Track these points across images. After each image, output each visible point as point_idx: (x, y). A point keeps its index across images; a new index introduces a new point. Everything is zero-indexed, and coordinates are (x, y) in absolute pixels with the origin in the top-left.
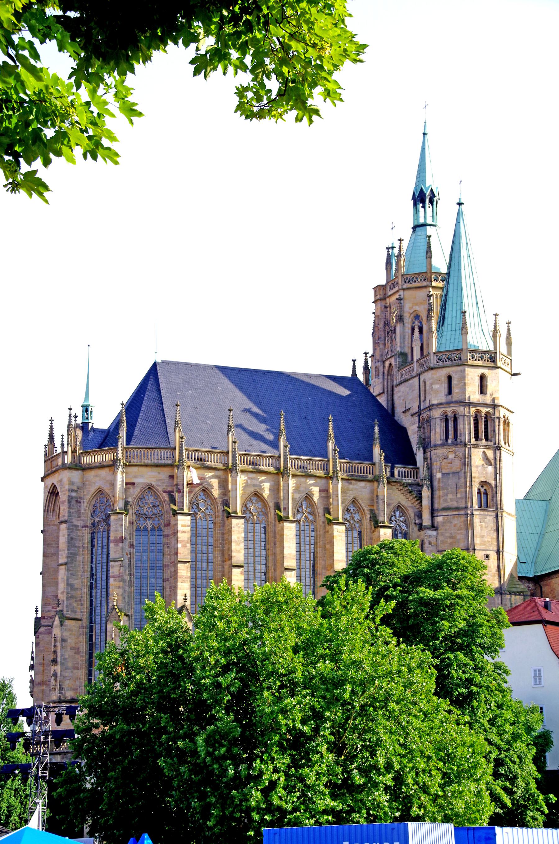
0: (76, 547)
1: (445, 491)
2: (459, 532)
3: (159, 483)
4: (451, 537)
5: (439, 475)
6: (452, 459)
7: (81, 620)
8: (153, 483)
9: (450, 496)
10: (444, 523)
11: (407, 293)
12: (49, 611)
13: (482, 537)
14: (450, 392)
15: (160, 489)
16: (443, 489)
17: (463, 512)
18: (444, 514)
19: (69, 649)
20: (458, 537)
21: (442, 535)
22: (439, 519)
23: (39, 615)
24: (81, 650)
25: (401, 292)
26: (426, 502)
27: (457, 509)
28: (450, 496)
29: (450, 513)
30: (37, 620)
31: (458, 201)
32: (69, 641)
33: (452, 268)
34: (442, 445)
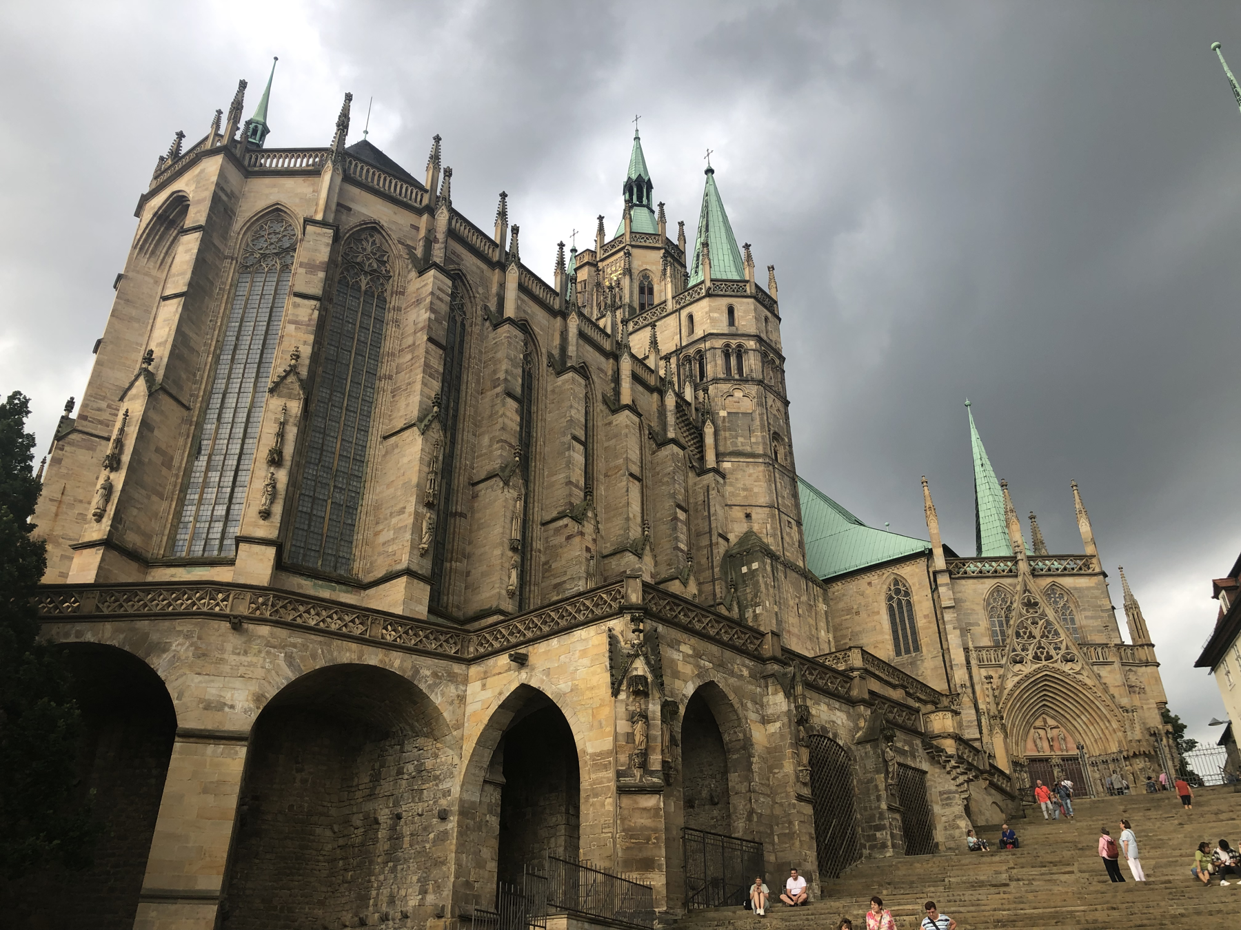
0: (208, 279)
1: (734, 433)
2: (756, 483)
3: (394, 228)
4: (745, 489)
5: (723, 413)
6: (739, 398)
7: (188, 409)
8: (383, 223)
9: (740, 439)
10: (733, 471)
11: (635, 252)
12: (99, 410)
13: (783, 497)
14: (732, 322)
15: (393, 236)
16: (730, 430)
17: (761, 460)
18: (733, 460)
19: (153, 448)
20: (756, 490)
21: (731, 485)
22: (726, 465)
23: (74, 415)
24: (176, 463)
25: (630, 248)
26: (709, 440)
27: (753, 455)
28: (740, 439)
29: (742, 460)
30: (64, 419)
31: (705, 168)
32: (156, 432)
33: (710, 219)
34: (725, 380)
